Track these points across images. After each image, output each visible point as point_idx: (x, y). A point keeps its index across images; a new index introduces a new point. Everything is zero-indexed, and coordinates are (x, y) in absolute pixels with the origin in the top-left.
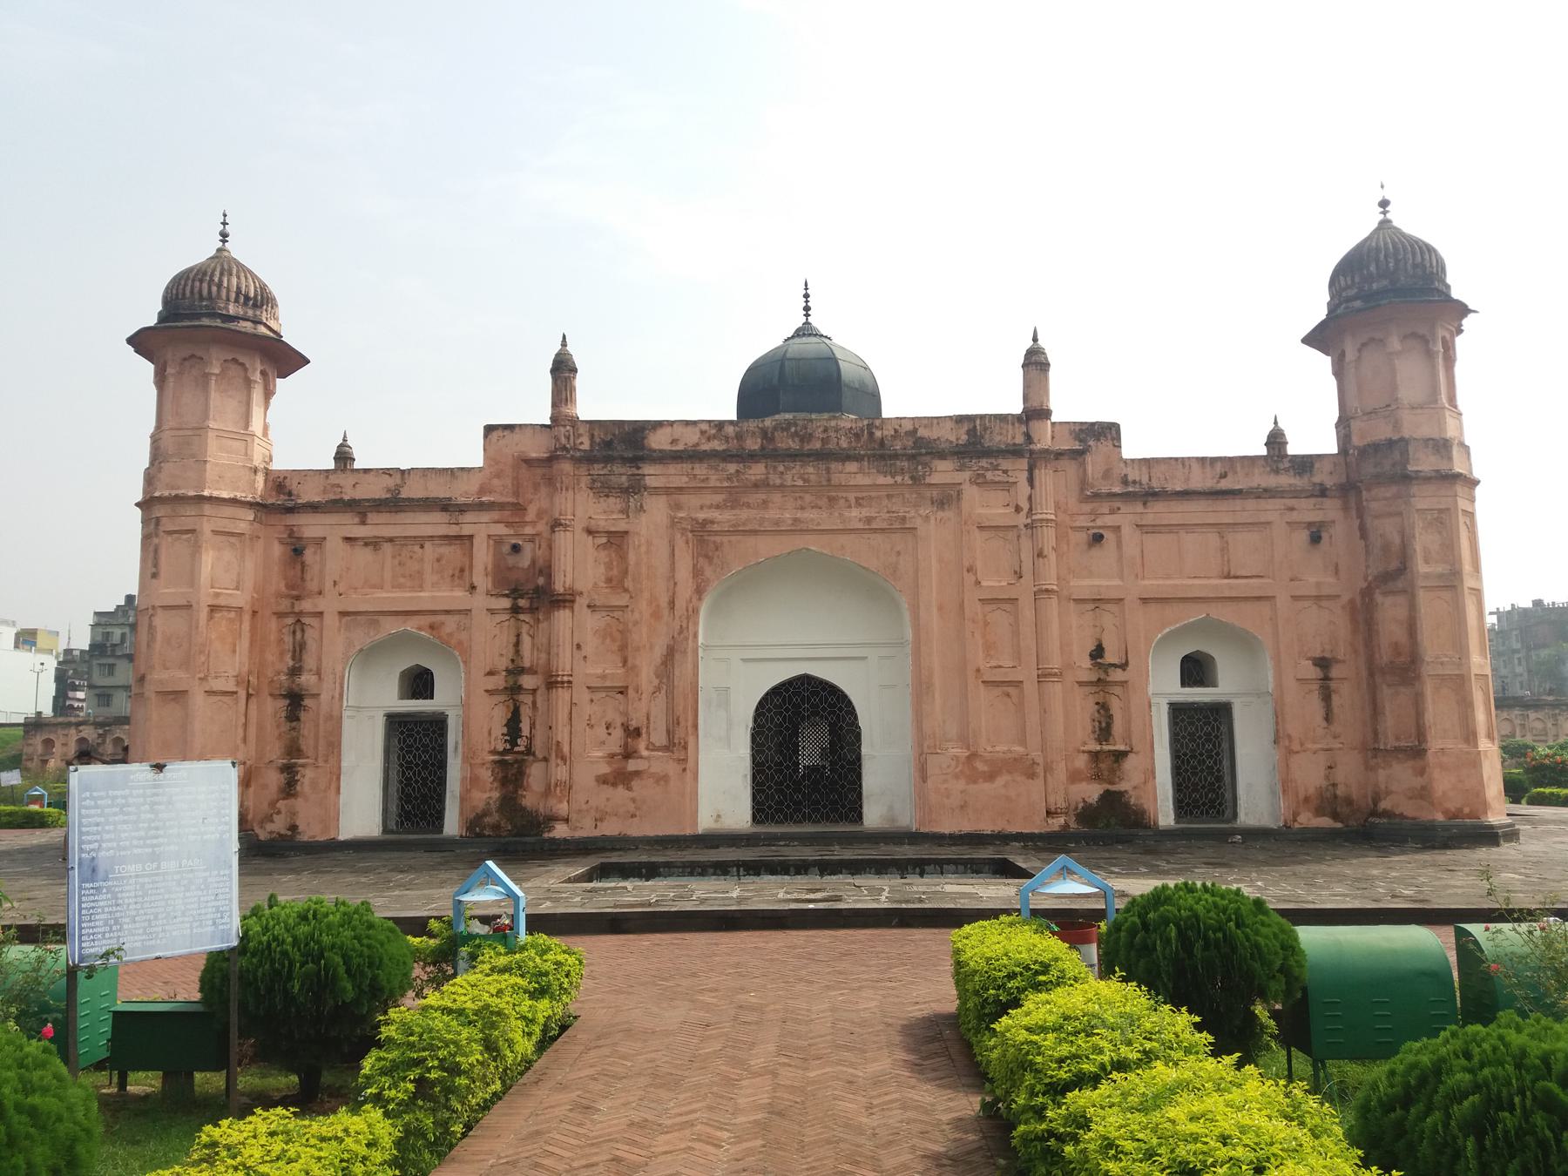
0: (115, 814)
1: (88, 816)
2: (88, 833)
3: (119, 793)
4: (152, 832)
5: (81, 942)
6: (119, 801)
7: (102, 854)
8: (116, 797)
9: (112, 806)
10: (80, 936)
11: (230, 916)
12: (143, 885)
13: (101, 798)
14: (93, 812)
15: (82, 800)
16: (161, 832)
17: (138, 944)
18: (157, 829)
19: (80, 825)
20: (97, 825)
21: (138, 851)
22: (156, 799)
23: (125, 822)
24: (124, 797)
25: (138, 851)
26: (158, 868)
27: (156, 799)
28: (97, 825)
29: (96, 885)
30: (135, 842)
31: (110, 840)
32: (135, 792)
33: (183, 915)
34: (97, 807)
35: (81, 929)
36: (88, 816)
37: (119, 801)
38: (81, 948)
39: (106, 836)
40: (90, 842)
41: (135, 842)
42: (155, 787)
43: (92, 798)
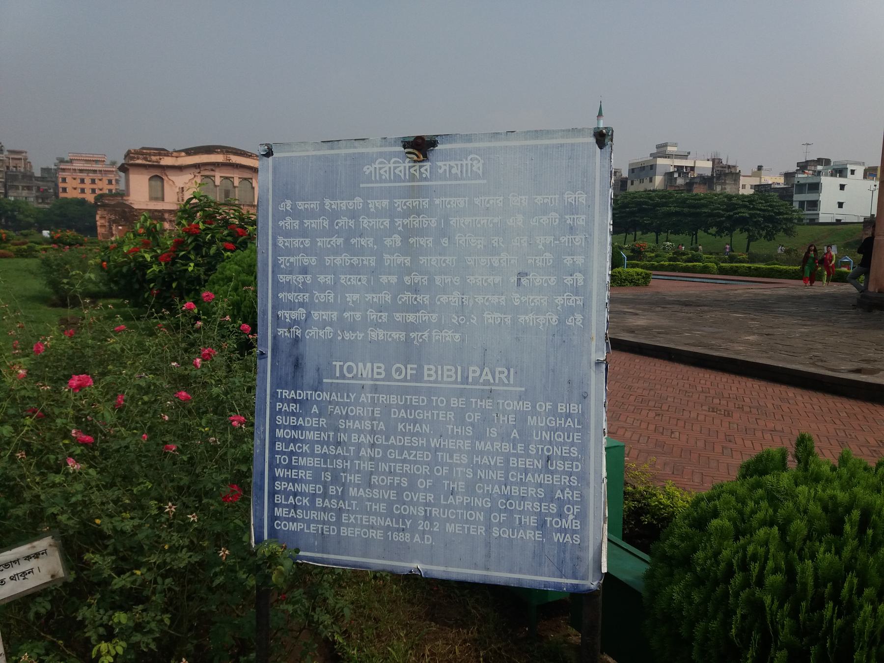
0: (336, 251)
1: (289, 252)
2: (289, 287)
3: (343, 205)
4: (407, 296)
5: (273, 505)
6: (343, 221)
7: (313, 332)
8: (334, 215)
9: (330, 232)
10: (273, 493)
11: (582, 516)
12: (388, 407)
13: (312, 215)
14: (296, 242)
15: (279, 216)
16: (424, 298)
17: (378, 535)
18: (415, 289)
19: (276, 265)
20: (304, 271)
21: (379, 334)
22: (414, 221)
23: (353, 269)
24: (354, 215)
25: (379, 334)
26: (418, 377)
27: (414, 221)
28: (304, 271)
29: (302, 395)
30: (372, 315)
31: (326, 306)
32: (373, 204)
33: (470, 490)
34: (303, 233)
35: (273, 478)
36: (289, 252)
37: (343, 221)
38: (273, 518)
39: (321, 297)
40: (292, 306)
41: (372, 315)
42: (414, 192)
43: (295, 214)
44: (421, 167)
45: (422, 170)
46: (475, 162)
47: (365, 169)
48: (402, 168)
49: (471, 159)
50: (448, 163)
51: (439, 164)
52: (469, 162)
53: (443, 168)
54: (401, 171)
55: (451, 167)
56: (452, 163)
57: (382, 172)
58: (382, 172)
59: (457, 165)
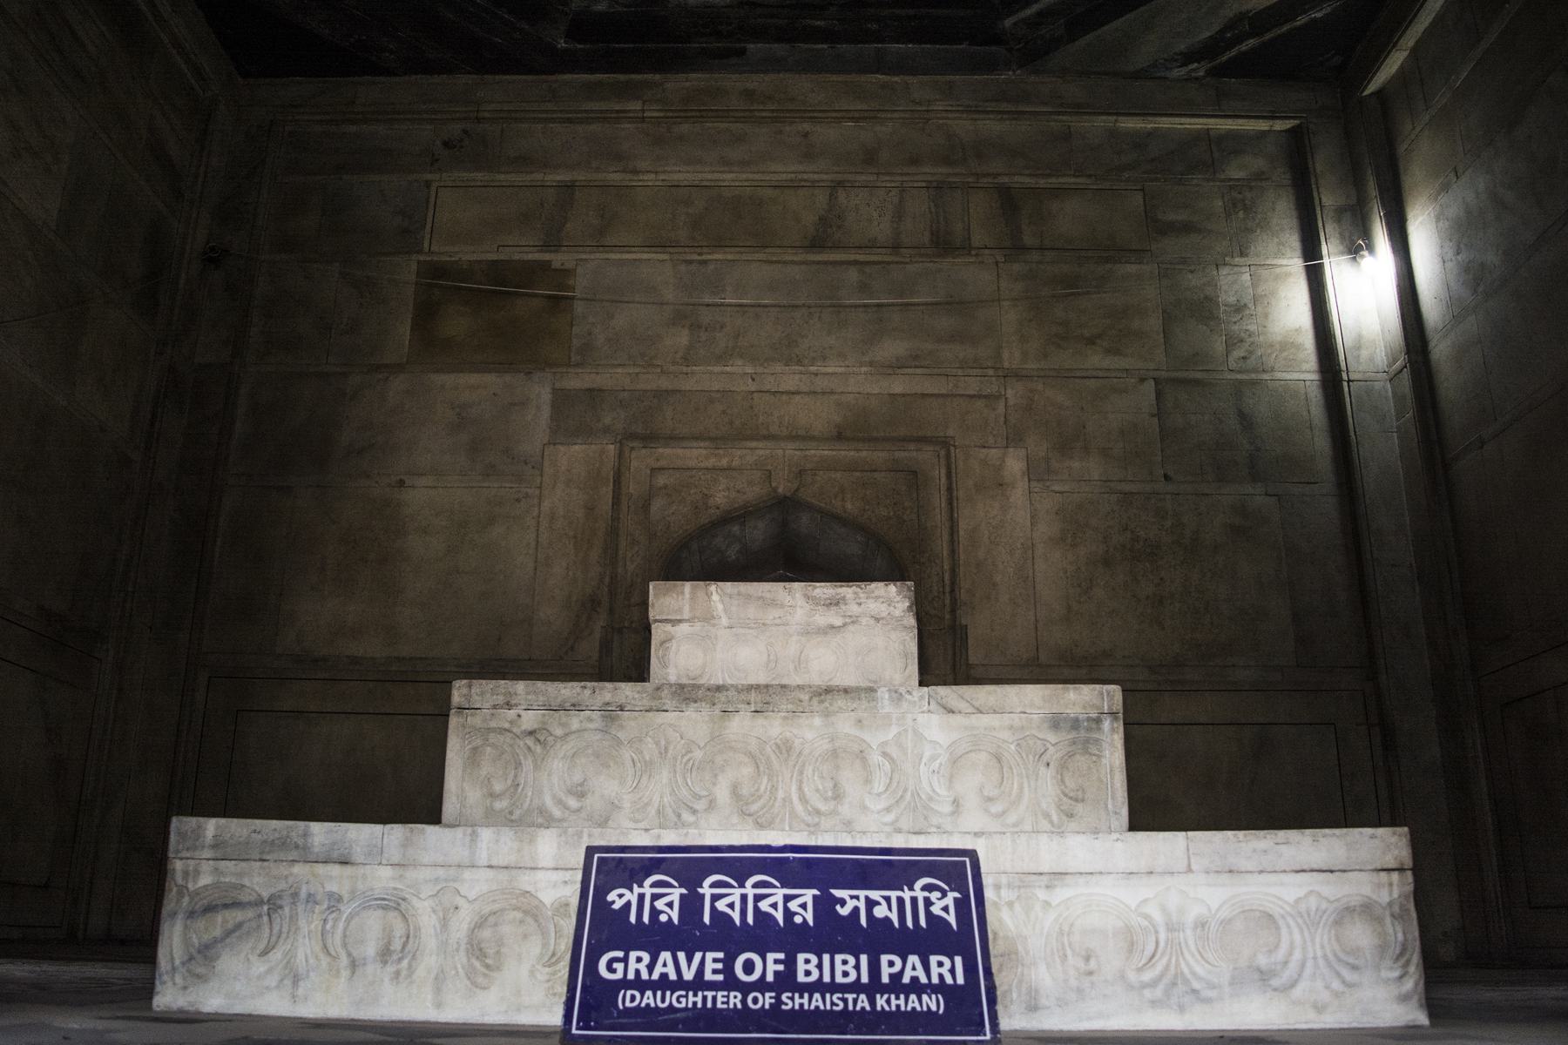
44: (787, 898)
45: (793, 906)
46: (935, 895)
47: (612, 896)
48: (736, 899)
49: (924, 888)
50: (862, 893)
51: (838, 893)
52: (921, 895)
53: (851, 904)
54: (731, 906)
55: (871, 904)
56: (875, 895)
57: (660, 904)
58: (660, 904)
59: (888, 899)
